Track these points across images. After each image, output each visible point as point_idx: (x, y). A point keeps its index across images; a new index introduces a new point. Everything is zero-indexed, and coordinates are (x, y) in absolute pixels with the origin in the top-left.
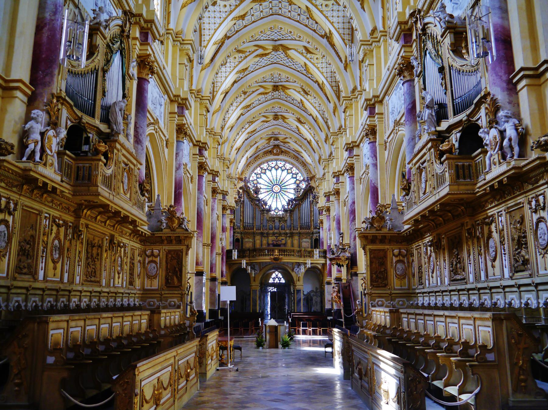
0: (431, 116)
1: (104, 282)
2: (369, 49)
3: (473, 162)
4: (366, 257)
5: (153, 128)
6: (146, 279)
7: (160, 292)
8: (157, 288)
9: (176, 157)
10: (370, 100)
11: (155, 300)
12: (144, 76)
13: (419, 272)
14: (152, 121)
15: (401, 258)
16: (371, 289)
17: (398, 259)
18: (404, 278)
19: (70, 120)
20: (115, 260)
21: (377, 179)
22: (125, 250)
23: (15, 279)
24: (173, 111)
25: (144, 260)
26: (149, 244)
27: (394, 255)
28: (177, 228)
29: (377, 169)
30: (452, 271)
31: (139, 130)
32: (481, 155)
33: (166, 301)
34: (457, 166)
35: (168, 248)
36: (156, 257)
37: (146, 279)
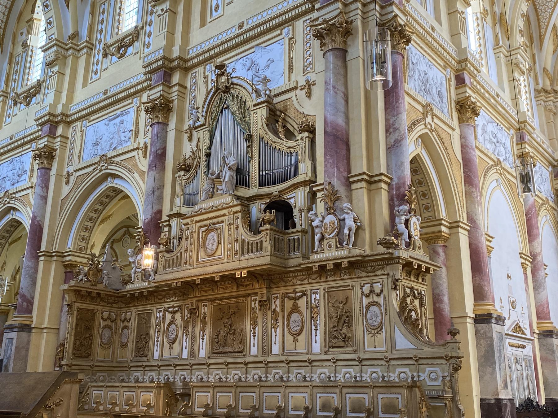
0: (231, 179)
2: (63, 53)
3: (286, 238)
4: (73, 317)
10: (55, 116)
13: (137, 342)
15: (110, 323)
16: (72, 359)
17: (106, 323)
18: (109, 348)
21: (43, 216)
27: (103, 318)
29: (46, 203)
30: (217, 343)
32: (300, 234)
34: (275, 237)
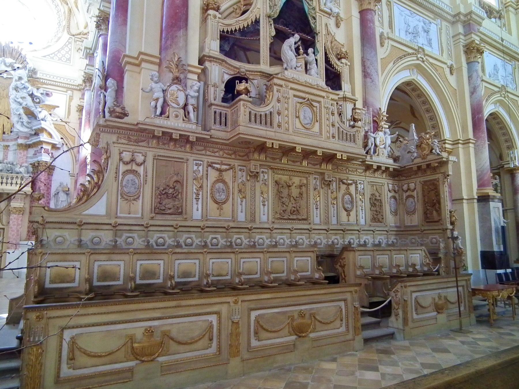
1: (317, 220)
5: (415, 58)
6: (406, 216)
7: (419, 229)
8: (416, 224)
9: (469, 80)
11: (416, 237)
12: (365, 7)
14: (410, 51)
19: (227, 74)
20: (336, 198)
22: (356, 188)
23: (152, 218)
24: (457, 33)
25: (402, 196)
26: (405, 178)
28: (428, 155)
31: (366, 64)
33: (428, 238)
35: (422, 179)
36: (413, 191)
37: (405, 215)
